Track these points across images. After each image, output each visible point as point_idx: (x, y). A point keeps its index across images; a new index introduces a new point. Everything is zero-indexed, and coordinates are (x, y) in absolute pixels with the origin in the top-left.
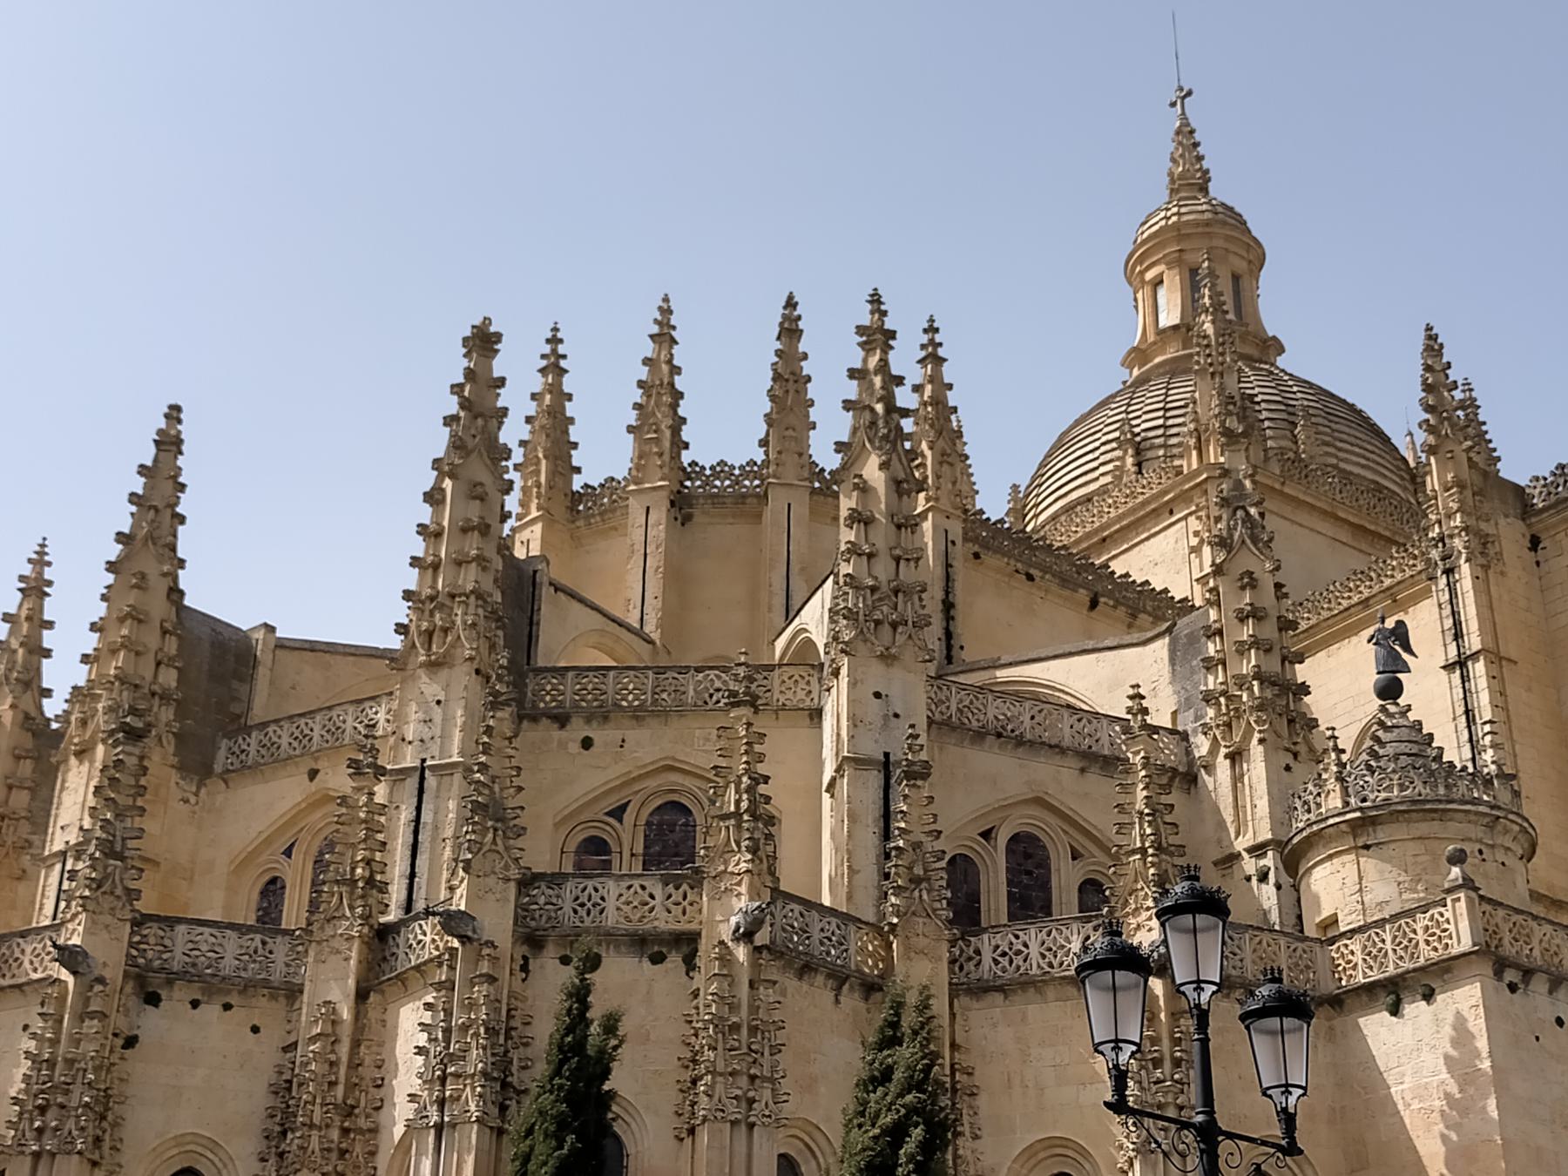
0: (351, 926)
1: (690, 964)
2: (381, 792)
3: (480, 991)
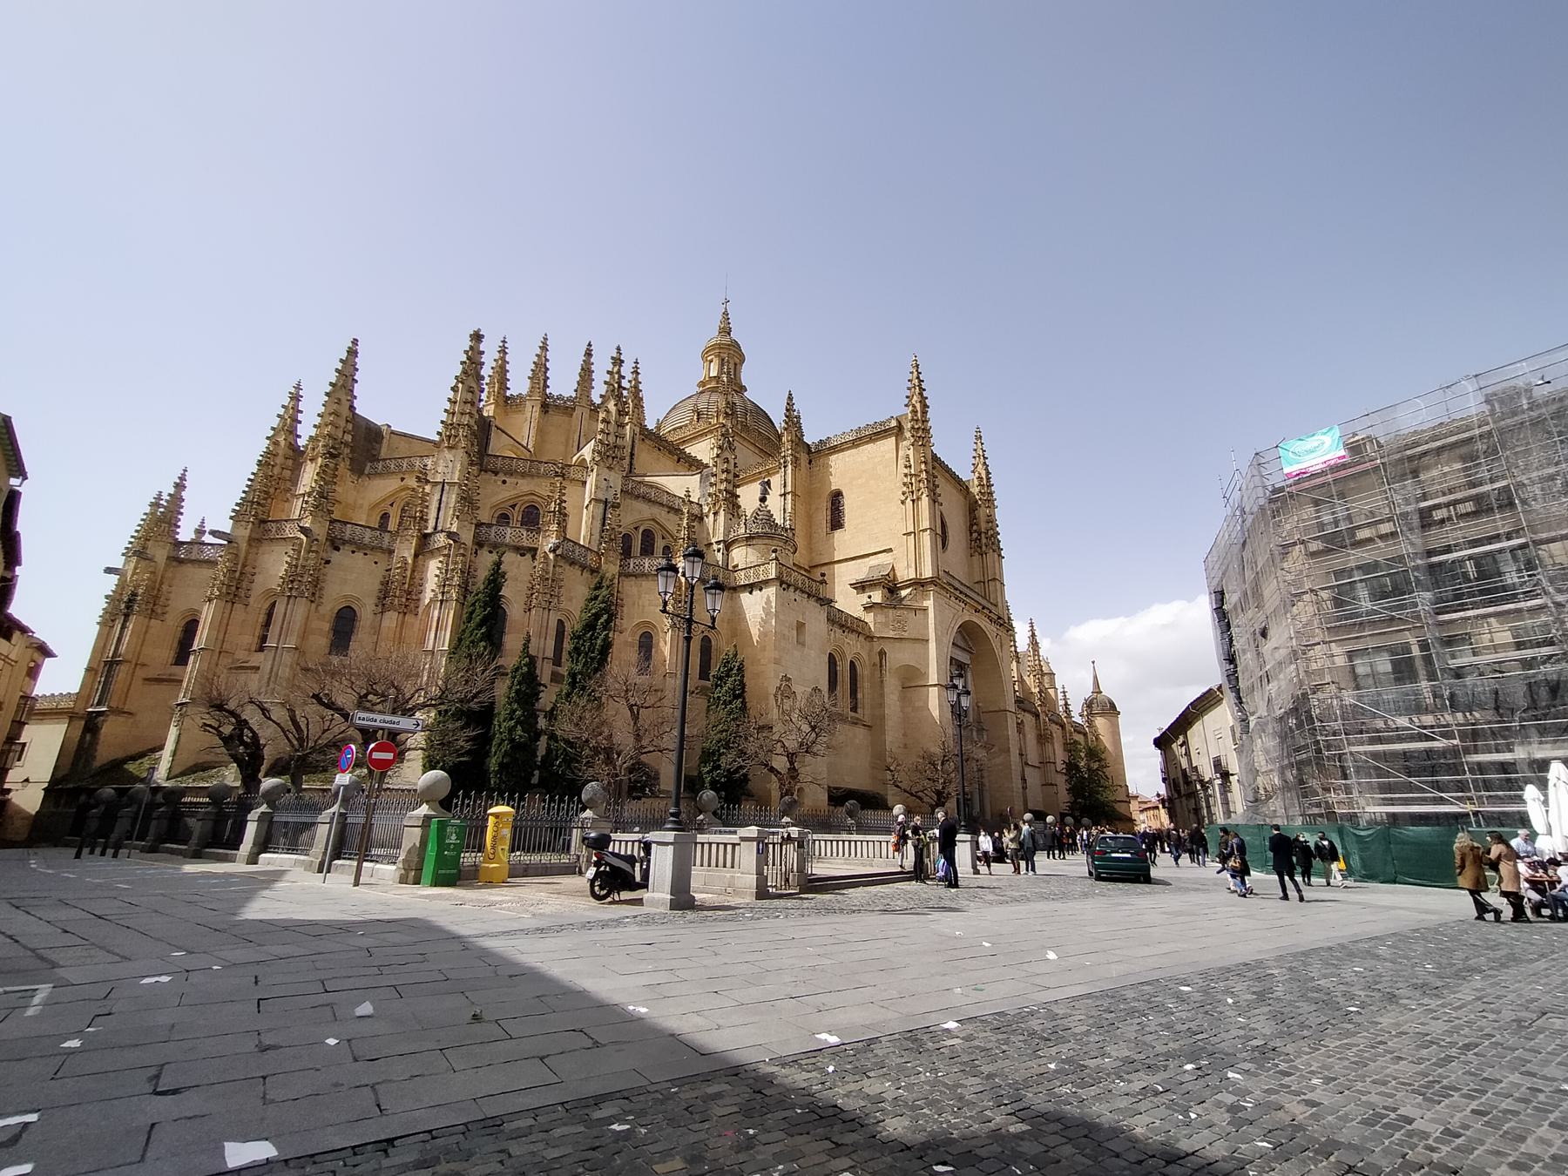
0: (413, 532)
1: (534, 558)
2: (428, 488)
3: (459, 559)
